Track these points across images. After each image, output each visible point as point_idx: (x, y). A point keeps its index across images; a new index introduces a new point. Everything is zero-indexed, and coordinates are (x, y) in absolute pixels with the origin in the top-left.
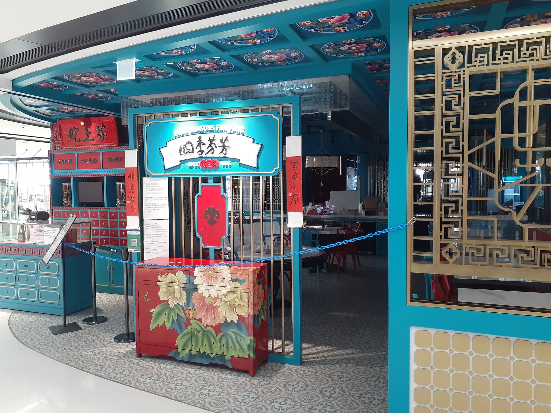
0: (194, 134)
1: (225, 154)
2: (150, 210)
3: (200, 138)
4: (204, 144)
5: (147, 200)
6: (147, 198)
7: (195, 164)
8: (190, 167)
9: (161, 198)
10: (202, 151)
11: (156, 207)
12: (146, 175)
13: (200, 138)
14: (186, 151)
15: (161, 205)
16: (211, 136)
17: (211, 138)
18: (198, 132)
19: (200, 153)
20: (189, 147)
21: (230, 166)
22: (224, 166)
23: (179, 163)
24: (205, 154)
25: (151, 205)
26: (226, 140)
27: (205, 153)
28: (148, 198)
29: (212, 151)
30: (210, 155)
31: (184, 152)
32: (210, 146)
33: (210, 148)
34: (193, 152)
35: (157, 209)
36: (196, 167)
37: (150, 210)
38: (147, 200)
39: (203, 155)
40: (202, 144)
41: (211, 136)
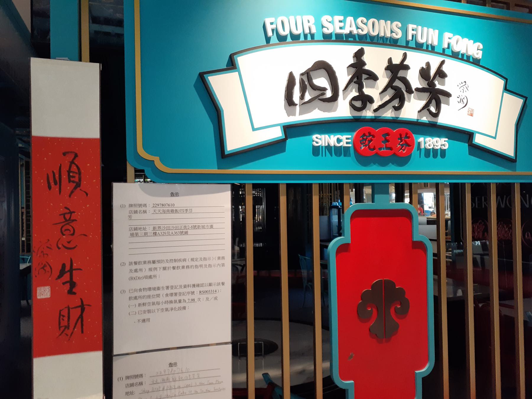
0: (334, 38)
1: (436, 115)
2: (146, 316)
3: (359, 54)
4: (373, 77)
5: (135, 275)
6: (134, 267)
7: (339, 141)
8: (316, 151)
9: (198, 263)
10: (366, 100)
11: (173, 298)
12: (130, 172)
13: (359, 54)
14: (307, 97)
15: (196, 290)
16: (396, 56)
17: (397, 61)
18: (351, 35)
19: (358, 104)
20: (322, 81)
21: (443, 153)
22: (427, 152)
23: (277, 134)
24: (375, 111)
25: (152, 293)
26: (441, 74)
27: (375, 105)
28: (138, 267)
29: (396, 103)
30: (389, 114)
31: (302, 97)
32: (390, 85)
33: (390, 93)
34: (334, 98)
35: (178, 305)
36: (338, 151)
37: (146, 316)
38: (135, 275)
39: (368, 113)
40: (364, 76)
41: (396, 56)
